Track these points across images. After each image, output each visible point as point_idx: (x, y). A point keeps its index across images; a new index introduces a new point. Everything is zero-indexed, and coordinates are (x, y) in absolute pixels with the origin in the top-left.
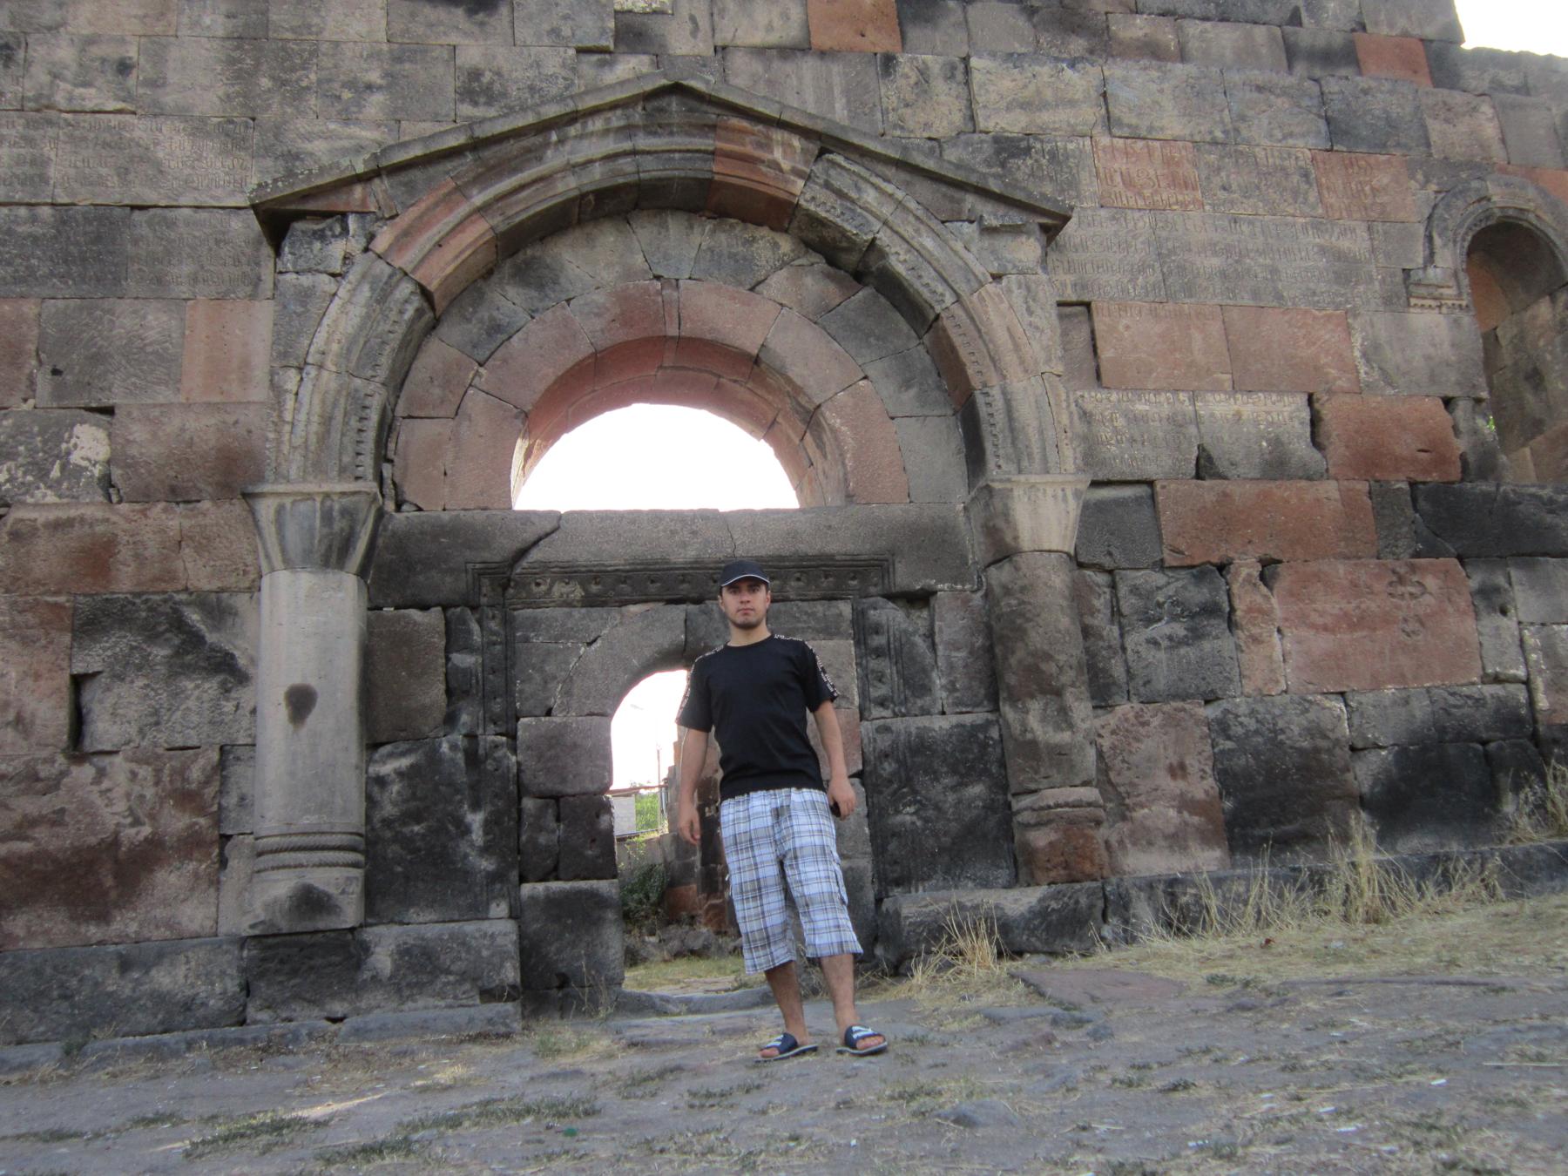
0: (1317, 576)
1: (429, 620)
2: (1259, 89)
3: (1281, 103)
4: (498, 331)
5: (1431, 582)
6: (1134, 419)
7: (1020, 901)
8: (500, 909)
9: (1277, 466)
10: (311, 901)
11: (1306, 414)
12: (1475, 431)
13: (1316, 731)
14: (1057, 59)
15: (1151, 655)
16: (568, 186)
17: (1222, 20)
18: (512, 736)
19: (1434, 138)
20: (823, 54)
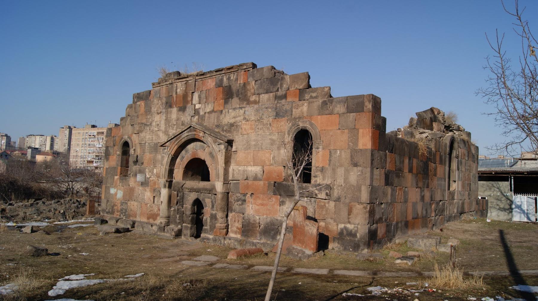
0: (258, 197)
1: (176, 193)
2: (267, 108)
3: (270, 110)
4: (183, 157)
5: (274, 199)
6: (239, 170)
7: (211, 237)
8: (180, 226)
9: (256, 178)
10: (161, 223)
11: (261, 170)
12: (287, 173)
13: (254, 221)
14: (240, 108)
15: (237, 206)
16: (183, 140)
17: (267, 93)
18: (183, 207)
19: (293, 113)
20: (215, 112)
